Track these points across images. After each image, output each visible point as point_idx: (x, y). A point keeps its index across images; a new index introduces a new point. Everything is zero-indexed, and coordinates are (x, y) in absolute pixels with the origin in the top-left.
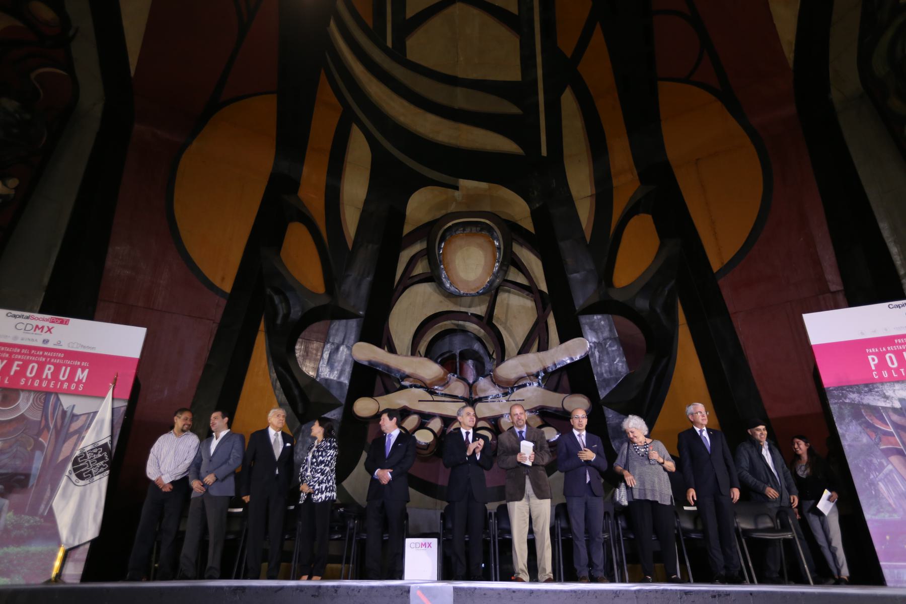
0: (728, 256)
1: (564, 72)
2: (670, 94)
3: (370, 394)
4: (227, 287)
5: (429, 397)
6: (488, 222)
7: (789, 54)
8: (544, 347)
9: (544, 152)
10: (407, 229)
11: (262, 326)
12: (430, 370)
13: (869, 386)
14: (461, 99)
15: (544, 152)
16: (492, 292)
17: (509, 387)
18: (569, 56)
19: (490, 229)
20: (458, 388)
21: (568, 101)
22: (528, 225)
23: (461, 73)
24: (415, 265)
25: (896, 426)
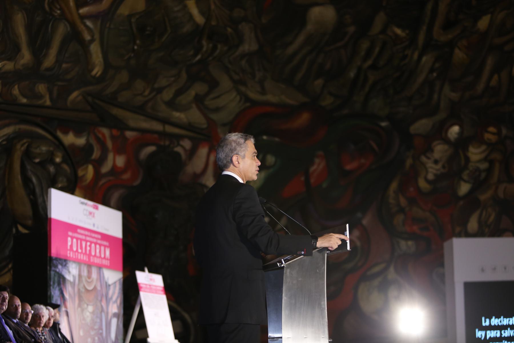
13: (64, 262)
25: (70, 295)
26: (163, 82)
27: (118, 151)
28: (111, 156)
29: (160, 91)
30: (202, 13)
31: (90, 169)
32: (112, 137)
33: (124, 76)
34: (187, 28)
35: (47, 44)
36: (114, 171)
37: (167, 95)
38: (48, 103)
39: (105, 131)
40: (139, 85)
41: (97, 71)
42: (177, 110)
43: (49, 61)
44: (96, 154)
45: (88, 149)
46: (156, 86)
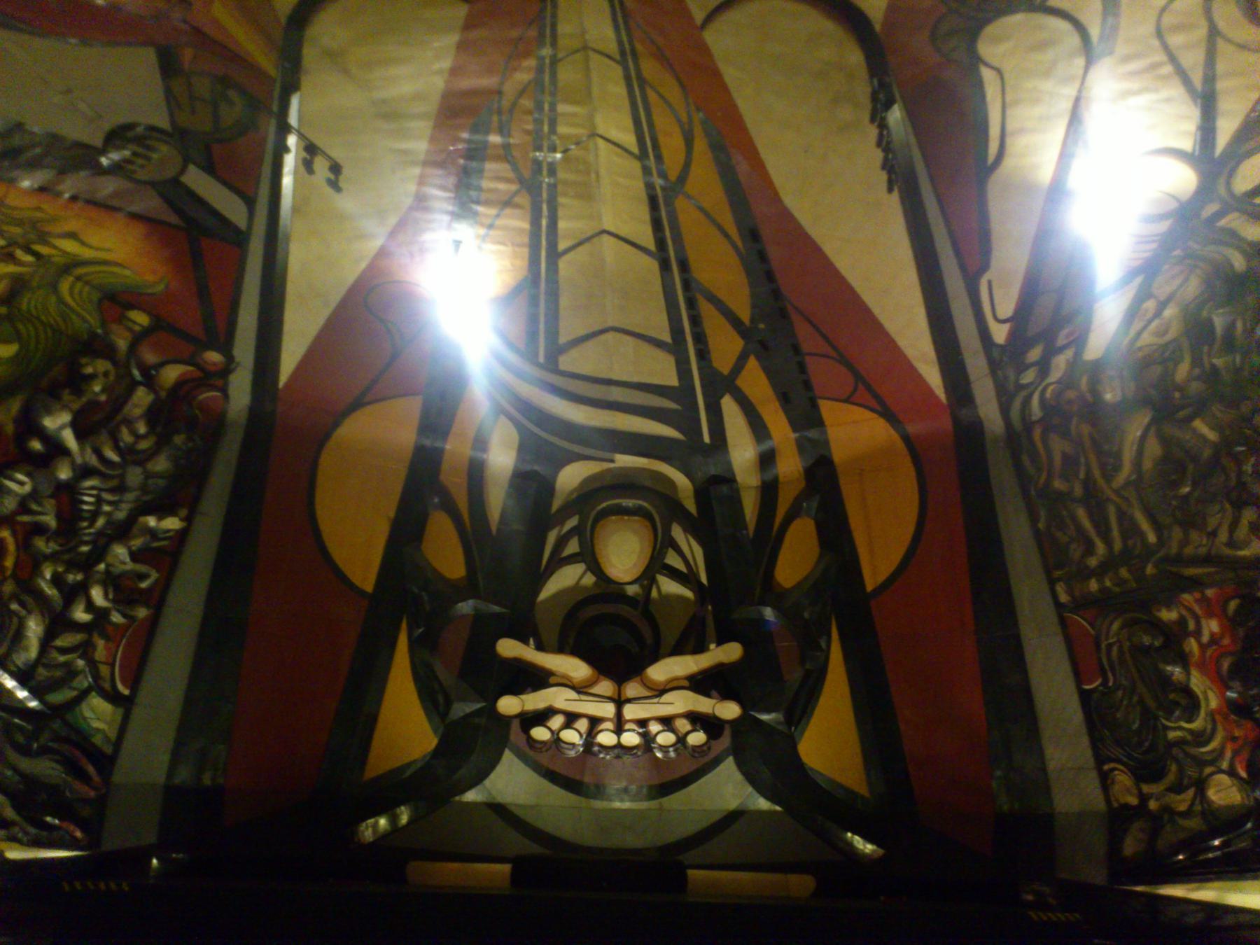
0: (881, 578)
1: (719, 385)
2: (827, 409)
3: (516, 690)
4: (369, 587)
5: (572, 695)
6: (645, 504)
7: (940, 393)
8: (700, 649)
9: (707, 439)
10: (556, 504)
11: (404, 625)
12: (577, 668)
14: (617, 394)
15: (707, 439)
16: (647, 577)
17: (660, 691)
18: (726, 371)
19: (647, 516)
20: (605, 687)
21: (729, 405)
22: (691, 506)
23: (615, 377)
24: (566, 545)
26: (1212, 522)
27: (1210, 615)
28: (1204, 622)
29: (1214, 534)
30: (1212, 428)
31: (1193, 641)
32: (1197, 601)
33: (1177, 533)
34: (1207, 453)
35: (1109, 529)
36: (1214, 640)
37: (1223, 536)
38: (1134, 585)
39: (1186, 597)
40: (1194, 535)
41: (1152, 538)
42: (1241, 549)
43: (1118, 546)
44: (1191, 625)
45: (1182, 622)
46: (1210, 529)
